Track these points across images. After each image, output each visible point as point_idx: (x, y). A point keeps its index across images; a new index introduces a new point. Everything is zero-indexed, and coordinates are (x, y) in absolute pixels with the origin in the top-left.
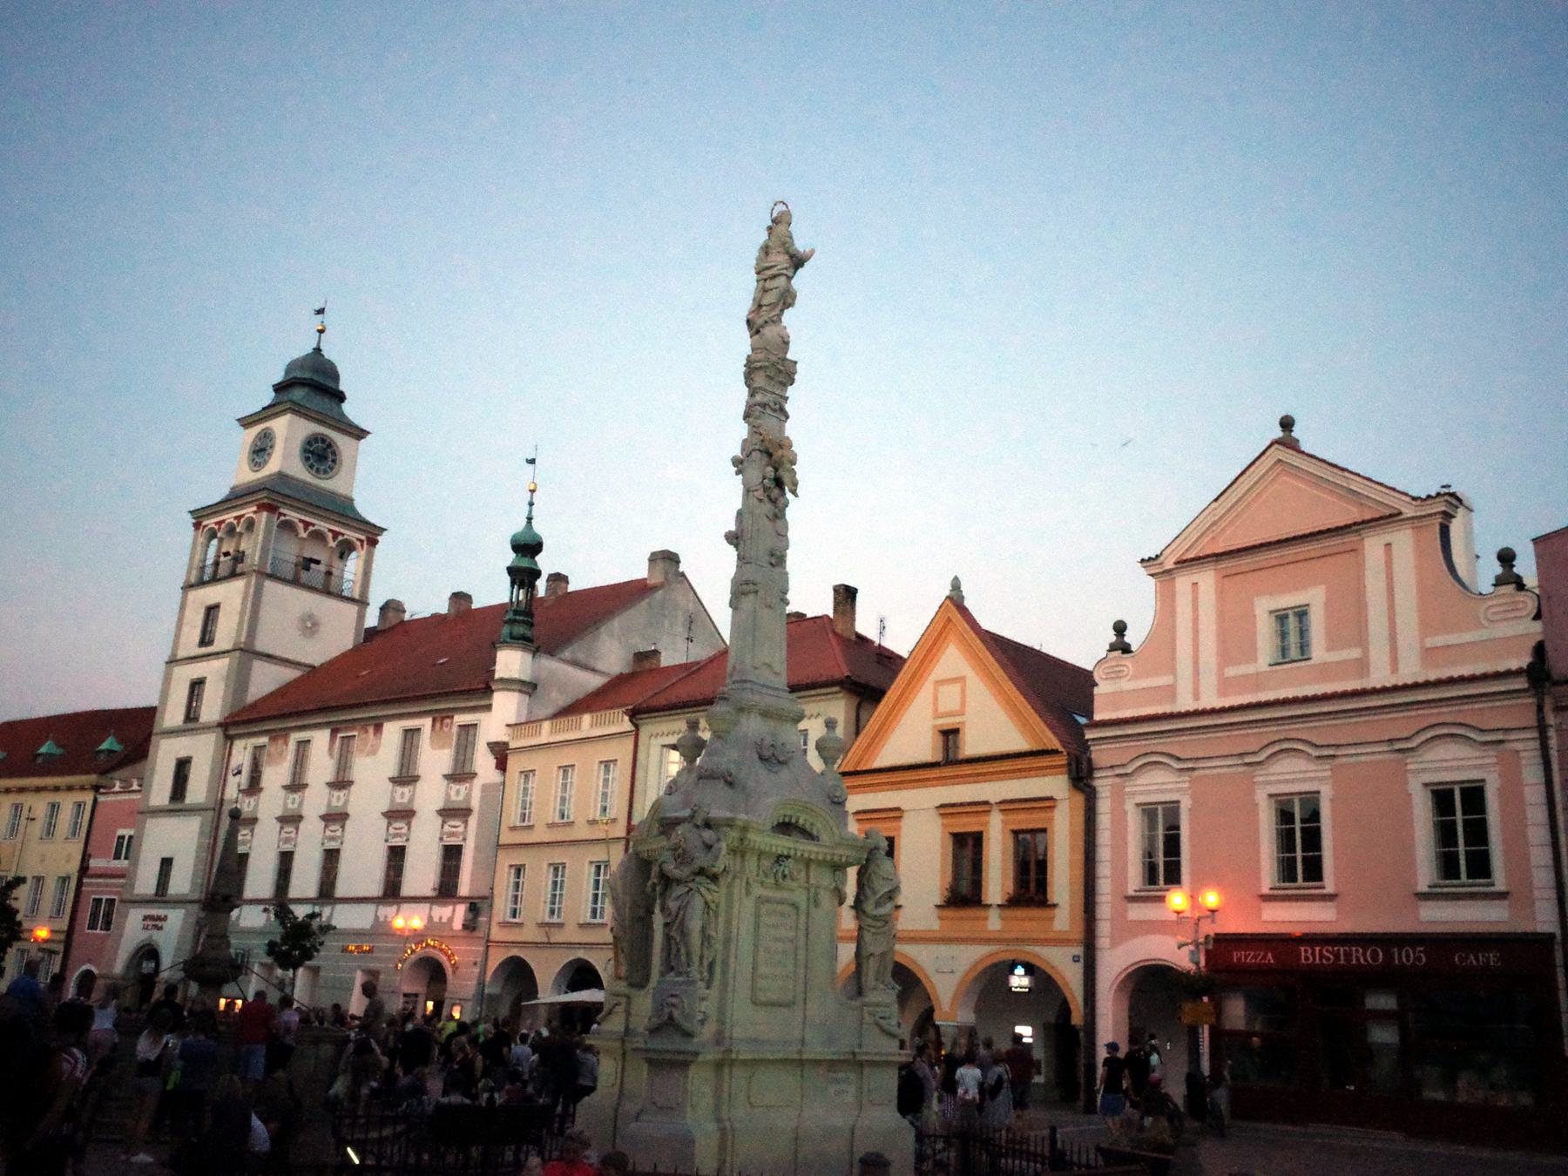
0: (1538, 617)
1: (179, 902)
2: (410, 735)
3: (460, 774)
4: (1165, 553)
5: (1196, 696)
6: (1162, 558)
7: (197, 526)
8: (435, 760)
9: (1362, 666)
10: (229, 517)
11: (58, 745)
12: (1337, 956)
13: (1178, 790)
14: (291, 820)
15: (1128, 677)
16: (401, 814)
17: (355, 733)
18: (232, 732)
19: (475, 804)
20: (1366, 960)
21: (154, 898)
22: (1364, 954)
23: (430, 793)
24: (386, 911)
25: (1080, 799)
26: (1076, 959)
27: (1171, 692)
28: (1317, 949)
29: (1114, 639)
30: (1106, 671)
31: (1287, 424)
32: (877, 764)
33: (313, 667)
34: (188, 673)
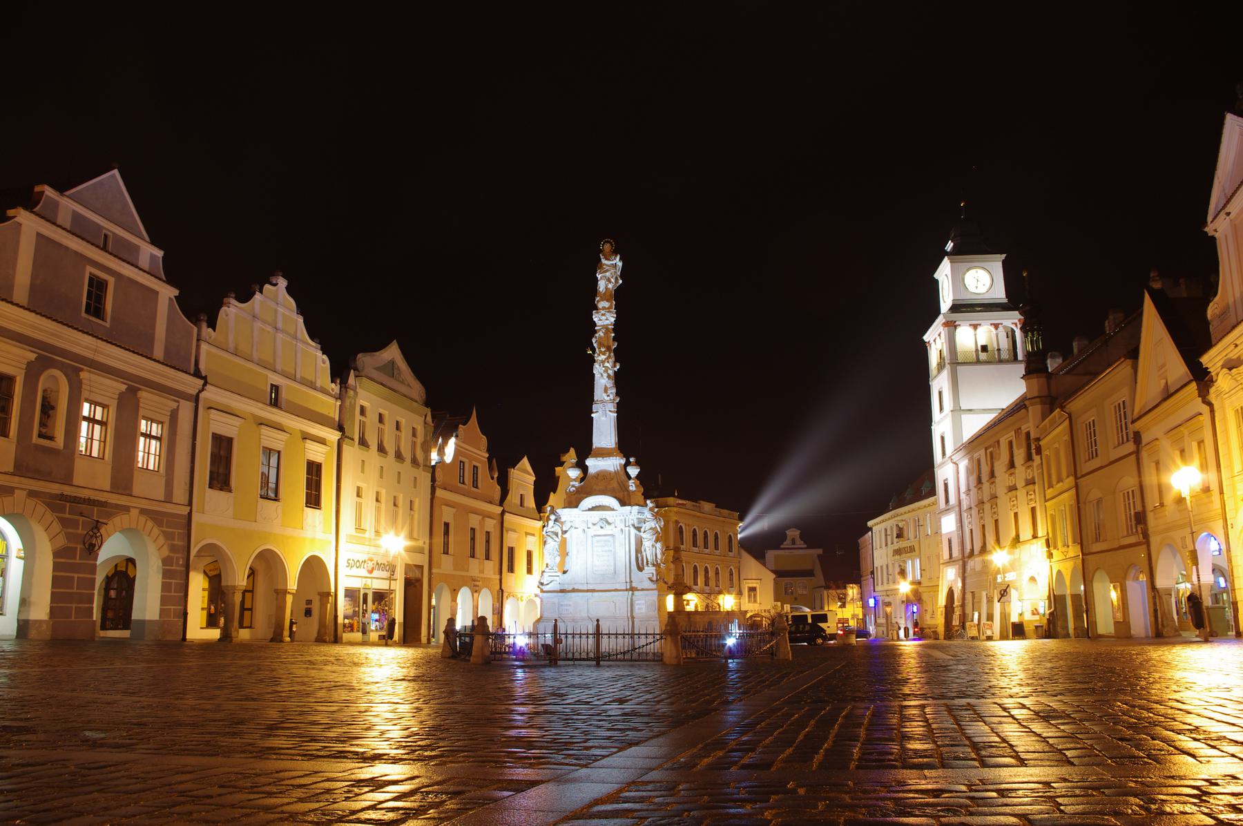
2: (1011, 443)
21: (948, 561)
33: (1003, 410)
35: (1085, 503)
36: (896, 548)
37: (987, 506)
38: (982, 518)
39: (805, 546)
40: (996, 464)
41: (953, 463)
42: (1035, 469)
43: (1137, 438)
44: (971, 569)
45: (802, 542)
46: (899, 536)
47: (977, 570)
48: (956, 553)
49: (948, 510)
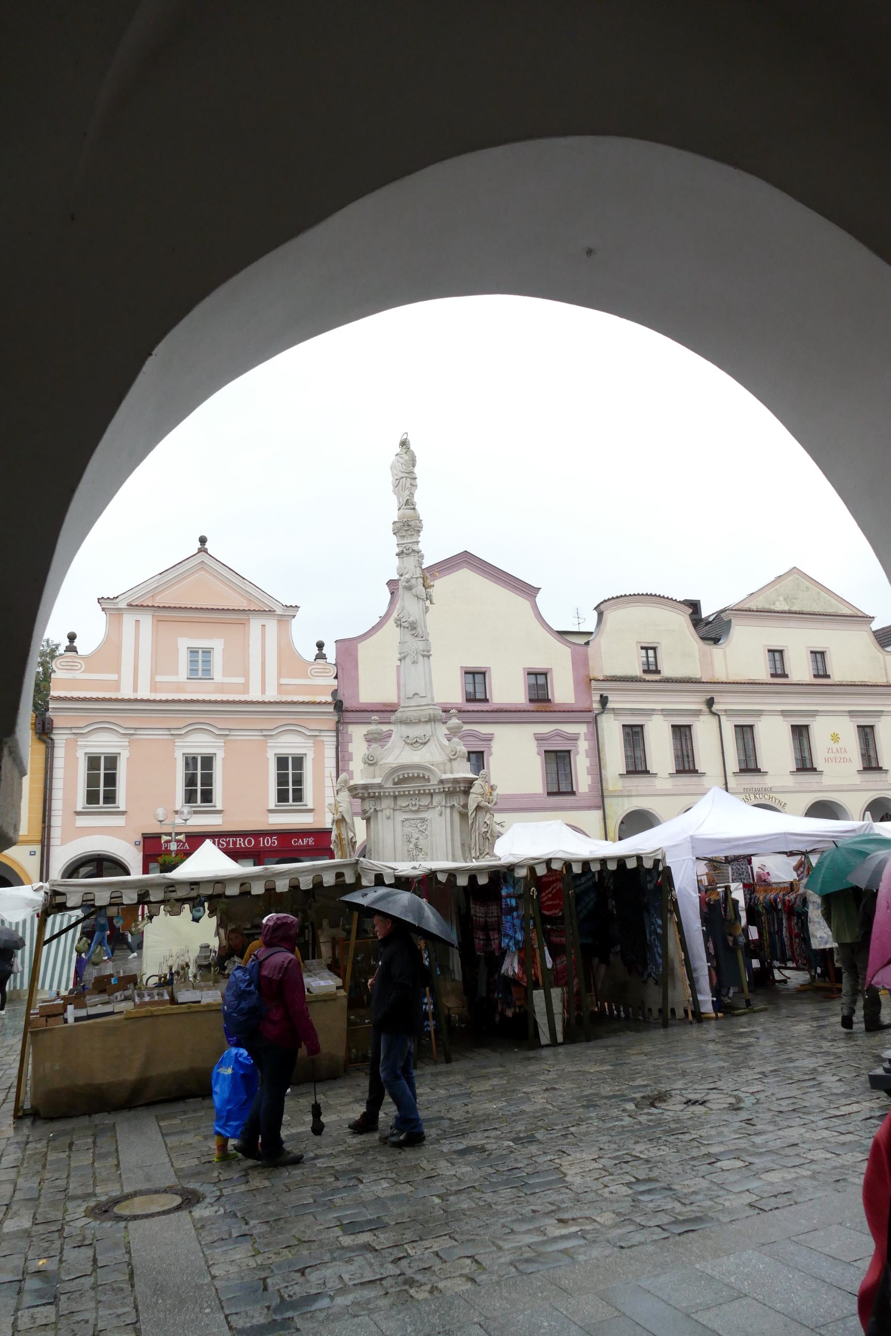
0: (336, 677)
4: (120, 598)
5: (135, 690)
6: (118, 600)
9: (245, 688)
12: (228, 843)
13: (120, 746)
15: (81, 671)
20: (244, 844)
22: (244, 842)
25: (42, 747)
26: (32, 854)
27: (117, 685)
28: (216, 840)
29: (68, 644)
30: (62, 664)
31: (203, 540)
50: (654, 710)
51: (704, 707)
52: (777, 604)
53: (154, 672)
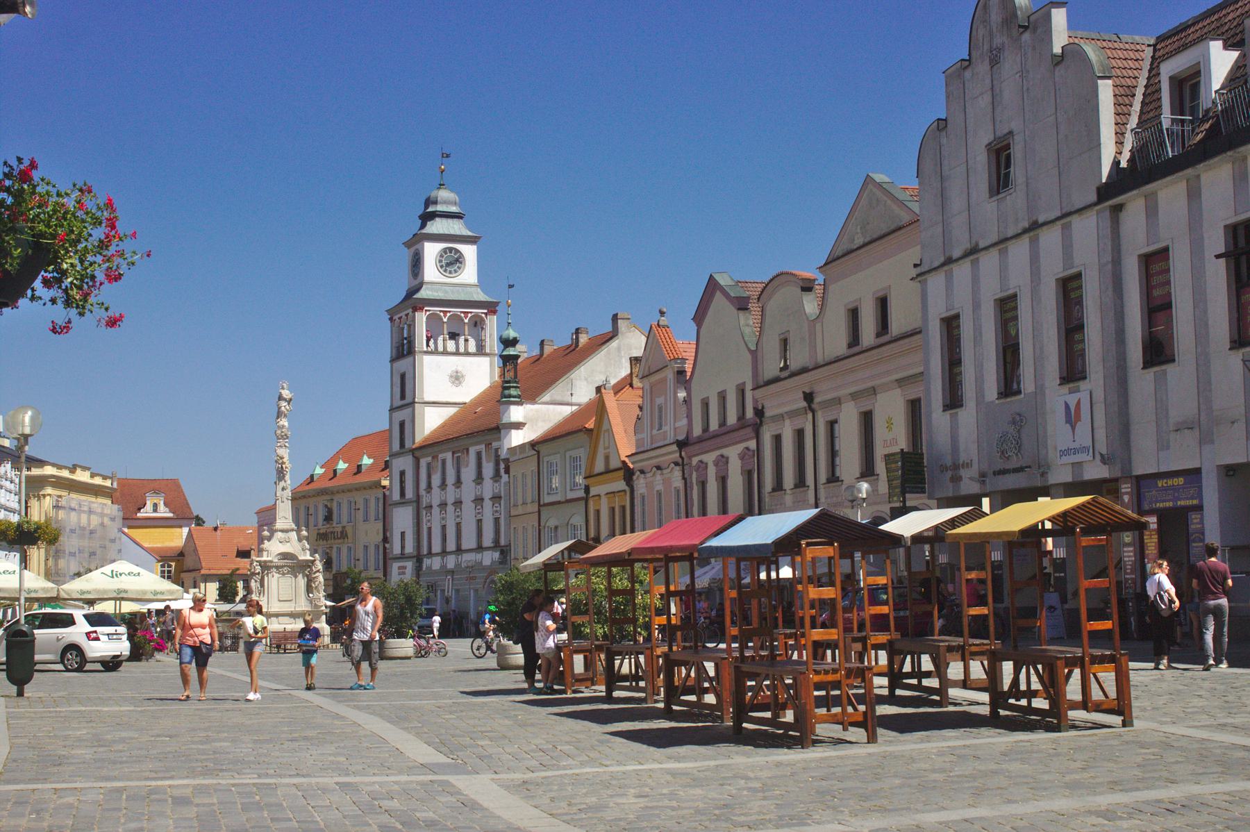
1: (409, 557)
2: (479, 454)
3: (497, 476)
7: (391, 319)
8: (488, 469)
10: (403, 314)
11: (369, 458)
14: (443, 505)
16: (479, 500)
17: (460, 454)
18: (417, 454)
19: (502, 495)
23: (488, 488)
24: (479, 556)
32: (595, 473)
33: (465, 403)
34: (399, 416)
35: (545, 527)
36: (321, 531)
37: (450, 508)
38: (443, 519)
39: (171, 515)
40: (463, 470)
41: (413, 456)
42: (502, 485)
43: (587, 489)
44: (427, 567)
45: (167, 509)
46: (328, 518)
47: (433, 568)
48: (409, 549)
49: (403, 503)
50: (782, 415)
51: (804, 404)
52: (856, 238)
53: (652, 430)
